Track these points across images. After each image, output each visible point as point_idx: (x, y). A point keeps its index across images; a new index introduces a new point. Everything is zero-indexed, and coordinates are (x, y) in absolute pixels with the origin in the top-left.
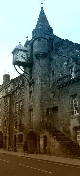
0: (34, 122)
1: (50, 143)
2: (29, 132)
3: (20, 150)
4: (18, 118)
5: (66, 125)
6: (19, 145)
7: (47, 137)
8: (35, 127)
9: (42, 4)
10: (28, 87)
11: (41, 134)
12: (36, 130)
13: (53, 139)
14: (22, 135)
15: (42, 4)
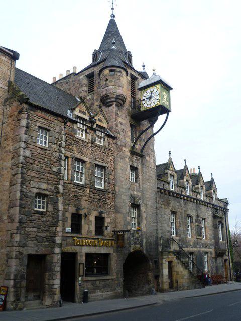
0: (143, 234)
1: (177, 273)
2: (132, 251)
3: (99, 294)
4: (85, 204)
5: (166, 247)
6: (96, 280)
7: (173, 264)
8: (146, 243)
9: (113, 9)
10: (126, 151)
11: (165, 257)
12: (149, 250)
13: (181, 266)
14: (107, 256)
15: (113, 9)
